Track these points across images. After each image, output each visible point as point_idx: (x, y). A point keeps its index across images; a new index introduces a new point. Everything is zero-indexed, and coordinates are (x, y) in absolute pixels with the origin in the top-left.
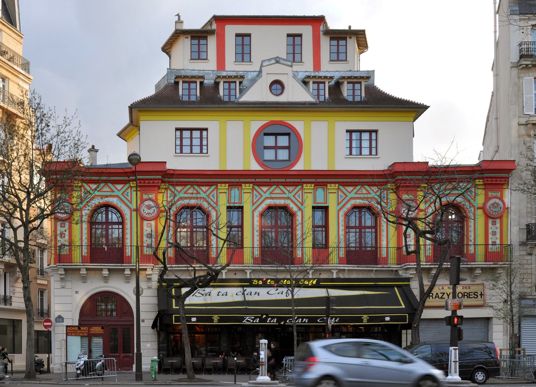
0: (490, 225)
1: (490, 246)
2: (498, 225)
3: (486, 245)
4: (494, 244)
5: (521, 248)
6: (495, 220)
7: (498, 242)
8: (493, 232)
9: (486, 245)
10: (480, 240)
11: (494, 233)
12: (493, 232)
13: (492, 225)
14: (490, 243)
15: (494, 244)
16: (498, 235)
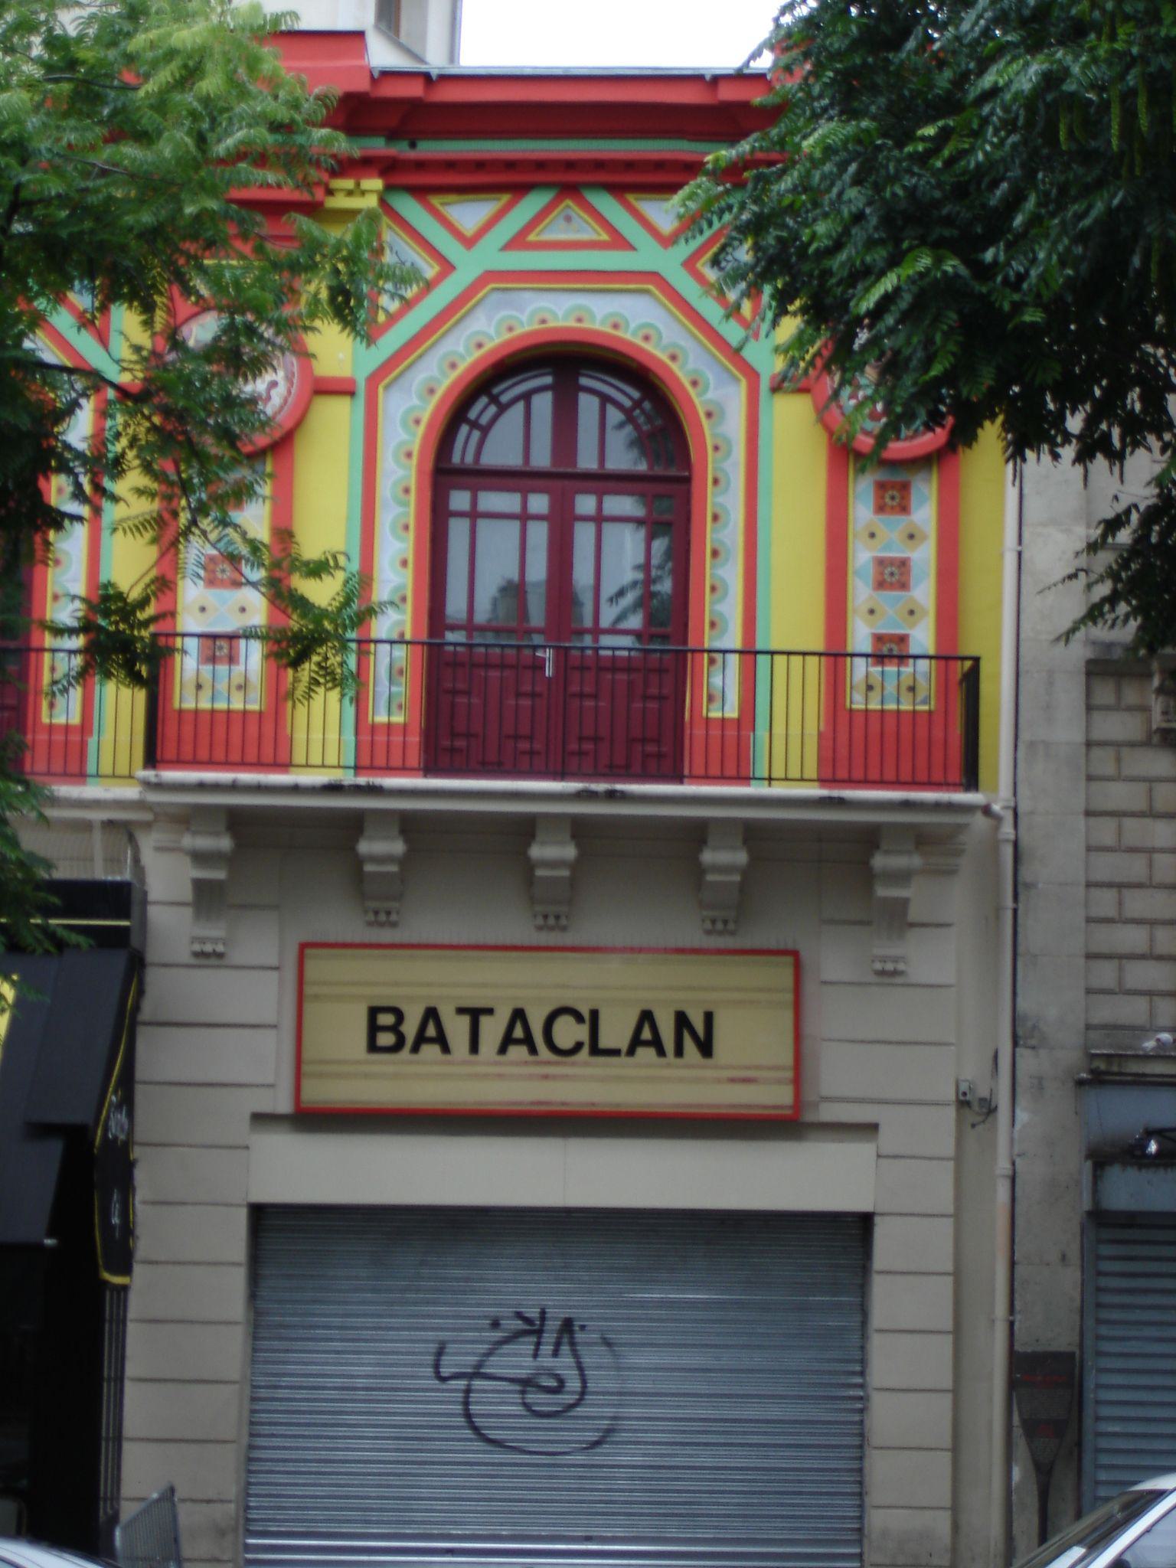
0: (862, 510)
1: (860, 669)
2: (925, 512)
3: (836, 656)
4: (890, 650)
5: (1105, 693)
6: (899, 477)
7: (923, 637)
8: (881, 562)
9: (836, 656)
10: (793, 617)
11: (893, 575)
12: (881, 562)
13: (880, 509)
14: (860, 636)
15: (890, 650)
16: (924, 591)
